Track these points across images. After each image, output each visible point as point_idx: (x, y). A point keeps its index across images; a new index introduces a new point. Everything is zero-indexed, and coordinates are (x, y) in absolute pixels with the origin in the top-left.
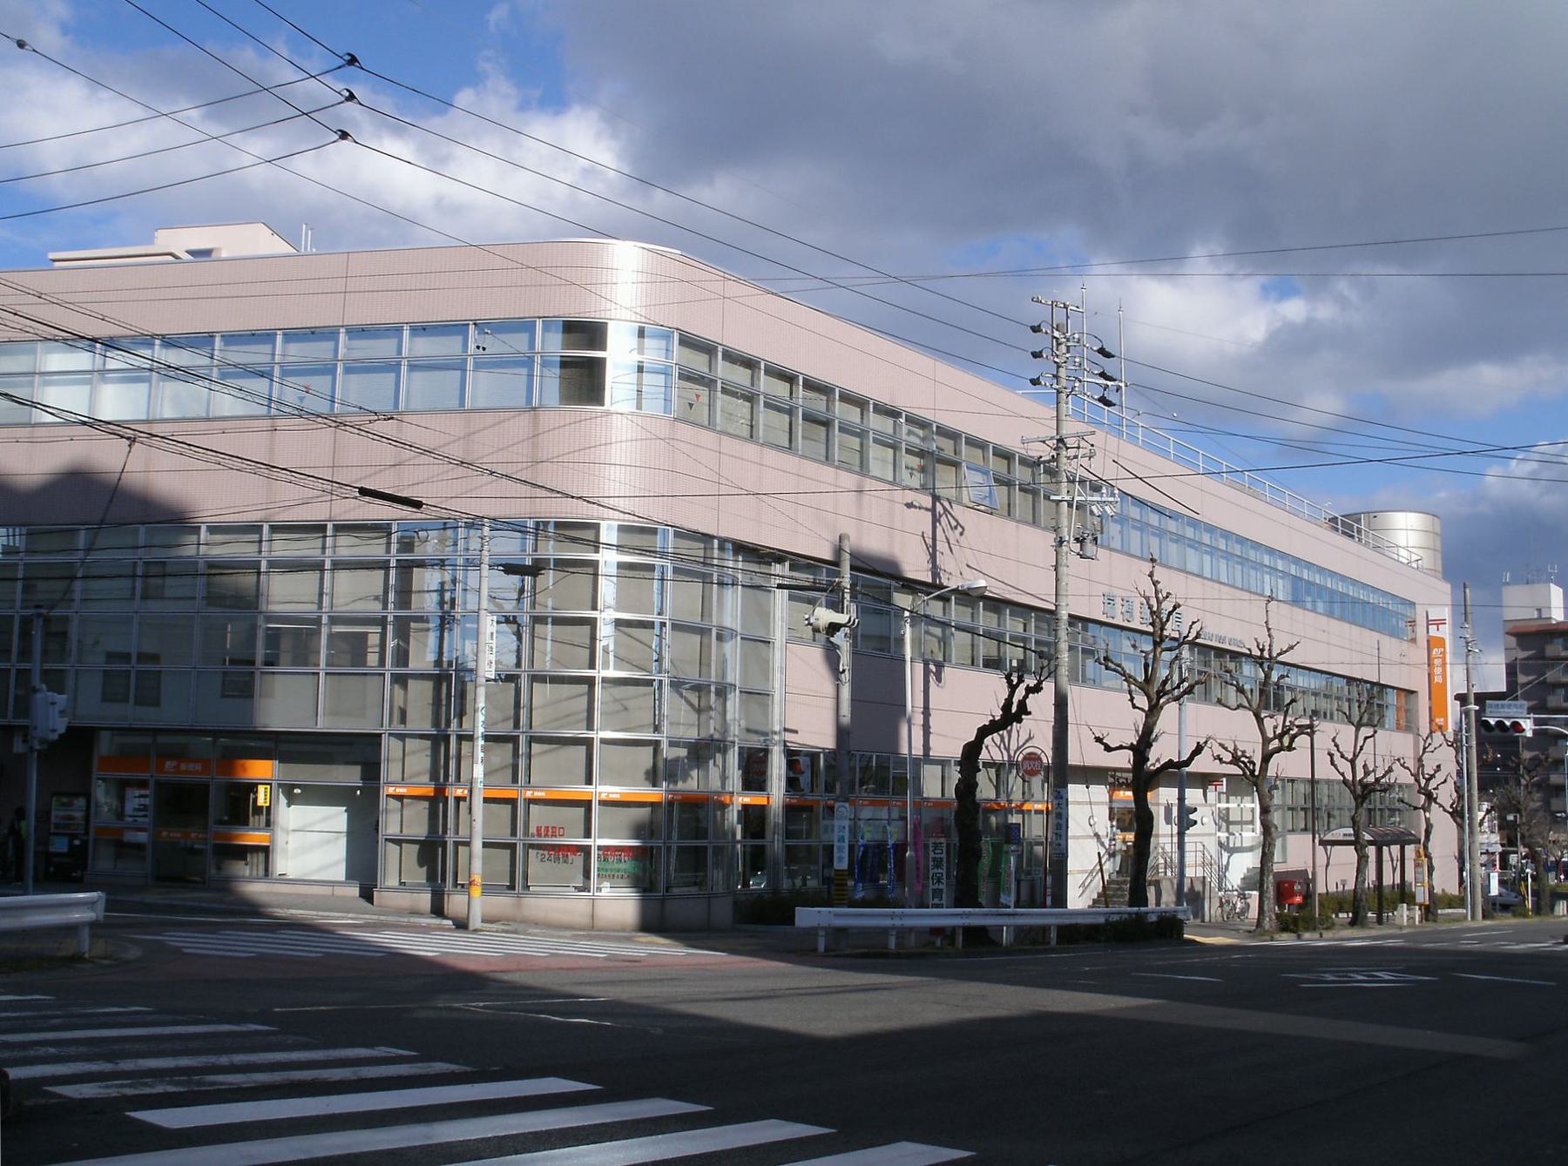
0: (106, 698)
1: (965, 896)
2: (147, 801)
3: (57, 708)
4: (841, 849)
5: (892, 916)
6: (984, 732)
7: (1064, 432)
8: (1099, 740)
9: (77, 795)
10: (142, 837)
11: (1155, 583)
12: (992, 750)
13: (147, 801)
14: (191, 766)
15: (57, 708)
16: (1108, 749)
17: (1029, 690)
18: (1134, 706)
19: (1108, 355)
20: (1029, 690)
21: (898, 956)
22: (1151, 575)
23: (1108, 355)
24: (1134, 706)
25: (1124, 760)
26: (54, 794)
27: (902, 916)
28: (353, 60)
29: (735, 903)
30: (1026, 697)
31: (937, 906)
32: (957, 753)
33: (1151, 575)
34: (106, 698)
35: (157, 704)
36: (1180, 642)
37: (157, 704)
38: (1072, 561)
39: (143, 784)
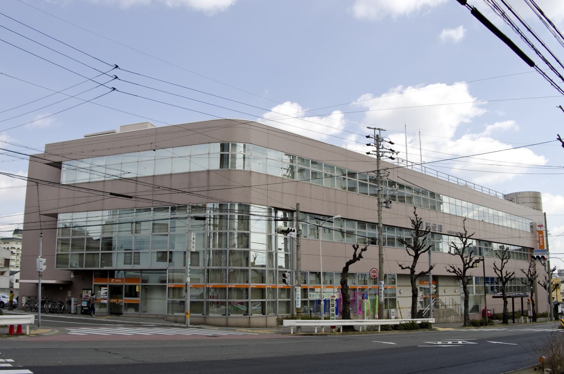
0: (125, 264)
1: (345, 315)
2: (107, 291)
3: (43, 263)
4: (298, 301)
5: (315, 322)
6: (348, 264)
7: (380, 168)
8: (400, 266)
9: (89, 290)
10: (106, 301)
11: (416, 215)
12: (352, 269)
13: (107, 291)
14: (118, 281)
15: (43, 263)
16: (403, 268)
17: (363, 250)
18: (410, 255)
19: (392, 143)
20: (363, 250)
21: (317, 335)
22: (415, 213)
23: (392, 143)
24: (410, 255)
25: (408, 272)
26: (83, 289)
27: (319, 322)
28: (117, 67)
29: (277, 319)
30: (361, 252)
31: (333, 319)
32: (341, 271)
33: (415, 213)
34: (125, 264)
35: (139, 264)
36: (426, 233)
37: (139, 264)
38: (384, 209)
39: (105, 286)
